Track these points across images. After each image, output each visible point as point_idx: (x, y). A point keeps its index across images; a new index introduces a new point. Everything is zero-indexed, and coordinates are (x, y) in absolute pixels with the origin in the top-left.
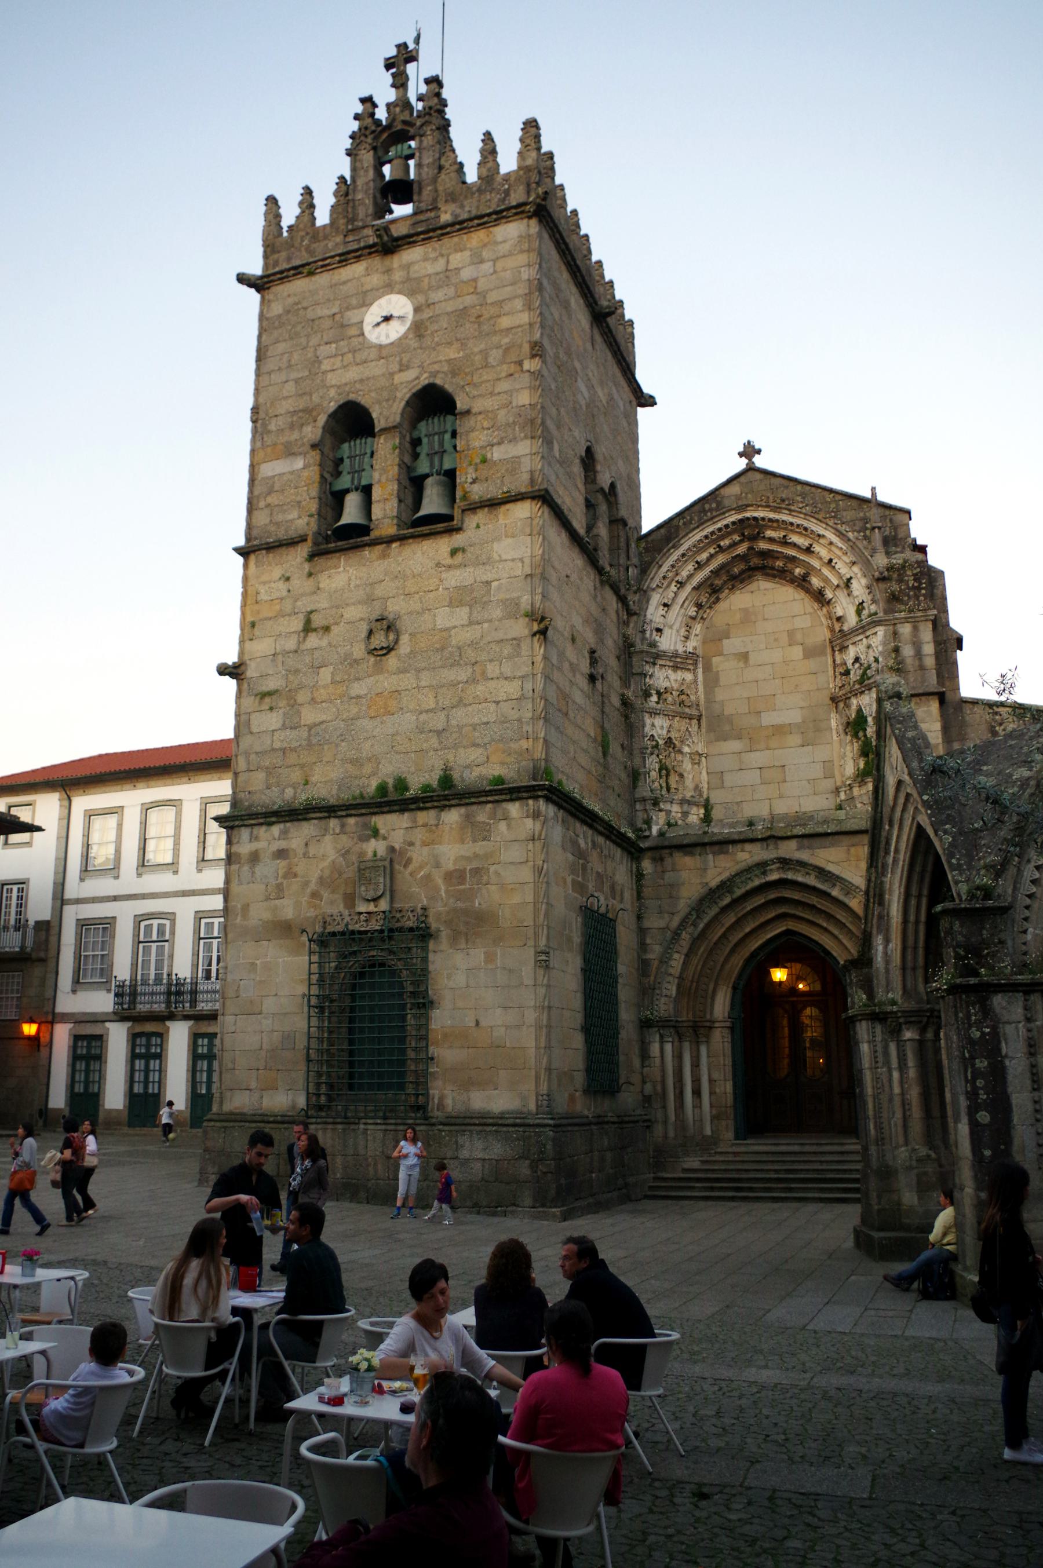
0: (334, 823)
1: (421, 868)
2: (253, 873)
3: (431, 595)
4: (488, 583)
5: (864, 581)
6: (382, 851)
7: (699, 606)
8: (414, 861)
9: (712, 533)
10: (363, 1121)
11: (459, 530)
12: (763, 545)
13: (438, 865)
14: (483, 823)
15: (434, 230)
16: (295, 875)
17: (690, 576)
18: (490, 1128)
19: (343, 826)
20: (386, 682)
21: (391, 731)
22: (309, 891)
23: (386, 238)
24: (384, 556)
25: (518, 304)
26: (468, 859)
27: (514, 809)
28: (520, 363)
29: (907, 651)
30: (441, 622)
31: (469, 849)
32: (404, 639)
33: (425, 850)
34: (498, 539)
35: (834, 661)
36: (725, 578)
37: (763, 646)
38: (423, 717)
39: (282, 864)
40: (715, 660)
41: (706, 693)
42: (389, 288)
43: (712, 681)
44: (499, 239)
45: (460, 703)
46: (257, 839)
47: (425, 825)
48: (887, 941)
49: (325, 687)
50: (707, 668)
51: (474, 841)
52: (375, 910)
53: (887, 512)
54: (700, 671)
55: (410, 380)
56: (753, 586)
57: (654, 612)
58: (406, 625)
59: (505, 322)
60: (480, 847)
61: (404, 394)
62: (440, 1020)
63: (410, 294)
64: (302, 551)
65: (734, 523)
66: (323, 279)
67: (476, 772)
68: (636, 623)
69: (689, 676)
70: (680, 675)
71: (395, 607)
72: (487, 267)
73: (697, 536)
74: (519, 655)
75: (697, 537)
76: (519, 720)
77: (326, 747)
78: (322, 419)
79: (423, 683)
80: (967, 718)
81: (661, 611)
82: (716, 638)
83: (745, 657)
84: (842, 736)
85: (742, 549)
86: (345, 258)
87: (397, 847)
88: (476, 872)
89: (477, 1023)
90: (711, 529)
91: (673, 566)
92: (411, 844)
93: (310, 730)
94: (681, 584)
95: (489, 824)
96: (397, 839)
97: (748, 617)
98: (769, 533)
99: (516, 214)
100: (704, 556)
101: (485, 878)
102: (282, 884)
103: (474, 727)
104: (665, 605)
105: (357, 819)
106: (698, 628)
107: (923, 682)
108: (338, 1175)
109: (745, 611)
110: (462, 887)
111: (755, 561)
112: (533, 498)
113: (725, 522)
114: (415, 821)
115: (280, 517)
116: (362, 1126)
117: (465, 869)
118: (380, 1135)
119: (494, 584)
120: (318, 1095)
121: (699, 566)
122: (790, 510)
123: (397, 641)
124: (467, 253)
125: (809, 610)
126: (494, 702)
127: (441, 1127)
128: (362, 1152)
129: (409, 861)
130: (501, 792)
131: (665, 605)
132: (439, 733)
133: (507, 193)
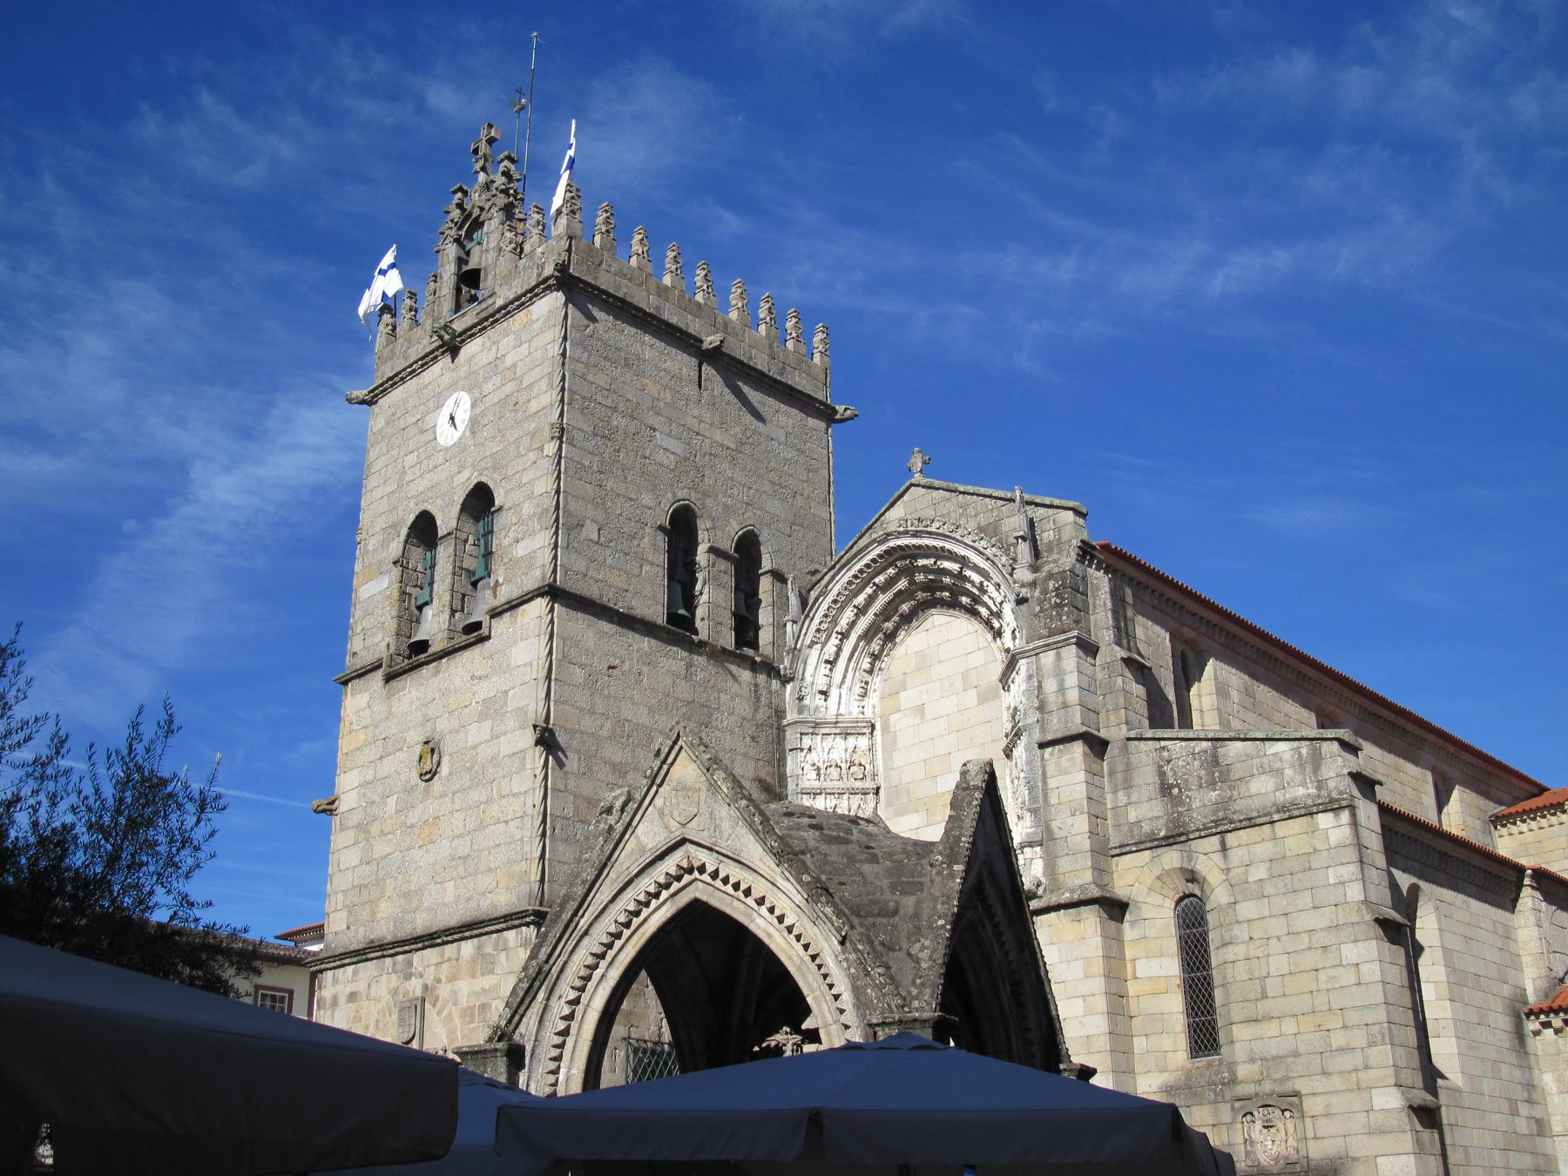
1: (444, 1006)
3: (466, 711)
4: (506, 692)
7: (876, 657)
9: (861, 571)
11: (488, 638)
12: (920, 578)
15: (486, 319)
17: (852, 625)
20: (432, 808)
21: (431, 860)
23: (447, 337)
24: (437, 672)
25: (543, 385)
28: (541, 449)
29: (1050, 686)
30: (472, 740)
32: (445, 760)
34: (515, 643)
36: (896, 618)
37: (938, 695)
40: (893, 718)
41: (885, 761)
42: (453, 387)
43: (891, 746)
44: (535, 317)
45: (482, 826)
47: (449, 960)
49: (391, 817)
50: (885, 729)
53: (1051, 511)
54: (878, 732)
55: (463, 483)
56: (928, 624)
57: (814, 672)
58: (448, 747)
59: (534, 406)
61: (460, 497)
63: (469, 391)
64: (378, 676)
65: (880, 556)
66: (412, 384)
68: (793, 688)
69: (863, 742)
70: (851, 739)
71: (443, 725)
72: (524, 349)
73: (845, 576)
74: (524, 769)
75: (846, 579)
76: (521, 840)
78: (404, 532)
80: (1133, 759)
81: (824, 669)
82: (892, 694)
83: (920, 709)
85: (902, 584)
86: (427, 360)
90: (857, 567)
91: (826, 616)
92: (439, 981)
94: (844, 636)
97: (924, 662)
98: (921, 562)
99: (544, 290)
100: (860, 599)
103: (489, 849)
104: (827, 662)
106: (877, 682)
107: (1067, 722)
109: (920, 654)
111: (920, 595)
112: (542, 595)
113: (870, 556)
114: (442, 956)
115: (369, 642)
121: (861, 611)
122: (930, 533)
123: (439, 764)
124: (512, 336)
125: (983, 643)
130: (511, 920)
131: (827, 662)
132: (465, 858)
133: (542, 266)
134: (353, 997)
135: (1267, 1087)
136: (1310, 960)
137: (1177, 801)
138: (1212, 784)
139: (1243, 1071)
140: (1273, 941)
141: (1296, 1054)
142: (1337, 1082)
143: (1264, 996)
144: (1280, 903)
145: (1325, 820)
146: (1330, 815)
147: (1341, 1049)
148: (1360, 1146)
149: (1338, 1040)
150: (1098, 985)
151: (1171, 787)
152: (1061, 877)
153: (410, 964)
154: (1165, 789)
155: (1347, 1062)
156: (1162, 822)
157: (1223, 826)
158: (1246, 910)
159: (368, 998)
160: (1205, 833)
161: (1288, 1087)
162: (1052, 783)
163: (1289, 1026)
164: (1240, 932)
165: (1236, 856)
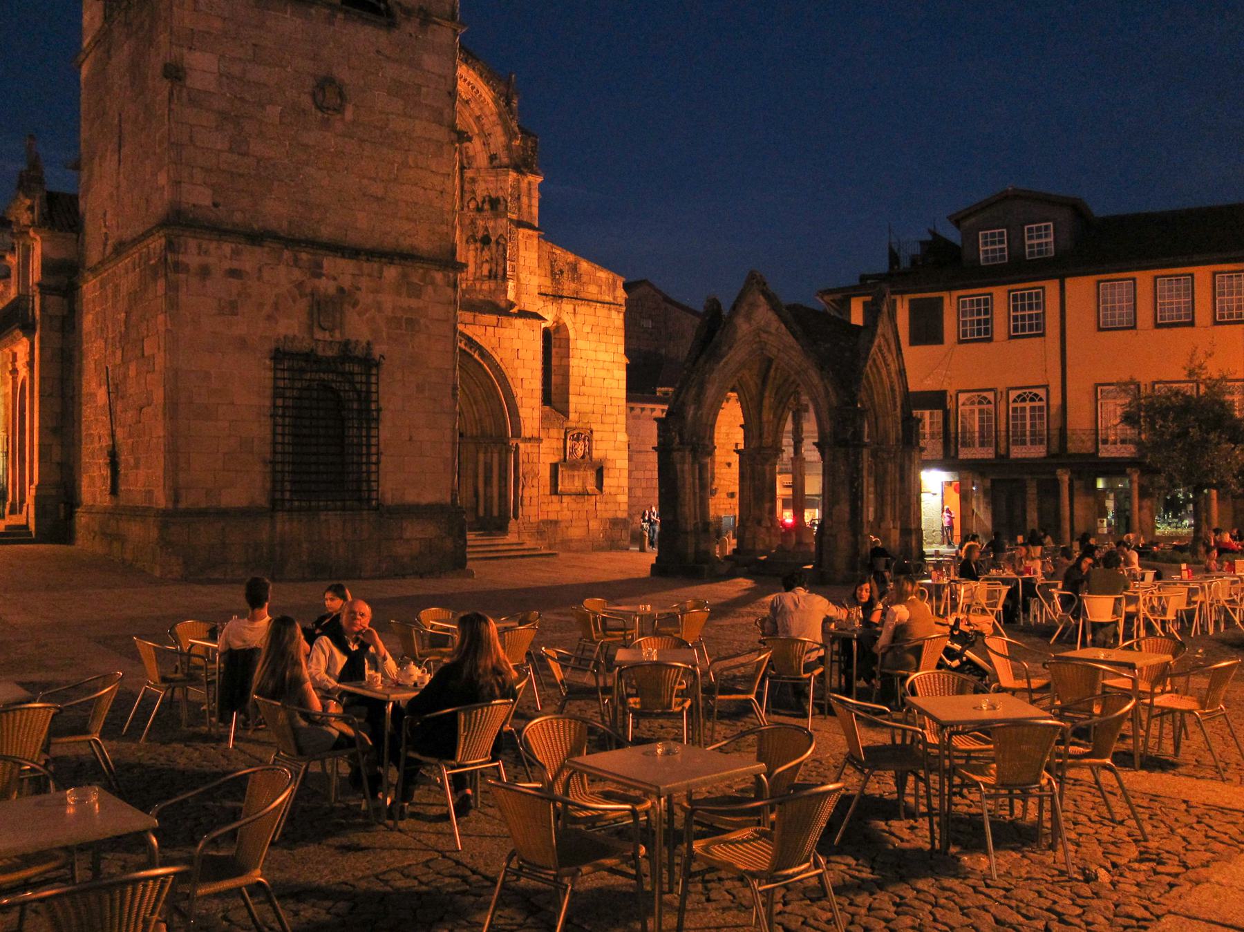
0: (287, 254)
1: (366, 311)
2: (204, 286)
6: (332, 290)
19: (296, 261)
27: (439, 276)
31: (406, 302)
33: (371, 296)
38: (365, 181)
39: (235, 281)
46: (206, 252)
51: (410, 297)
60: (414, 303)
62: (385, 432)
71: (342, 74)
77: (276, 183)
88: (410, 321)
96: (346, 282)
119: (424, 90)
120: (283, 492)
129: (355, 305)
134: (234, 273)
135: (580, 425)
138: (573, 280)
139: (572, 416)
142: (607, 427)
144: (593, 346)
148: (611, 455)
149: (609, 410)
154: (553, 273)
155: (612, 419)
159: (259, 279)
162: (522, 253)
163: (591, 400)
165: (580, 318)
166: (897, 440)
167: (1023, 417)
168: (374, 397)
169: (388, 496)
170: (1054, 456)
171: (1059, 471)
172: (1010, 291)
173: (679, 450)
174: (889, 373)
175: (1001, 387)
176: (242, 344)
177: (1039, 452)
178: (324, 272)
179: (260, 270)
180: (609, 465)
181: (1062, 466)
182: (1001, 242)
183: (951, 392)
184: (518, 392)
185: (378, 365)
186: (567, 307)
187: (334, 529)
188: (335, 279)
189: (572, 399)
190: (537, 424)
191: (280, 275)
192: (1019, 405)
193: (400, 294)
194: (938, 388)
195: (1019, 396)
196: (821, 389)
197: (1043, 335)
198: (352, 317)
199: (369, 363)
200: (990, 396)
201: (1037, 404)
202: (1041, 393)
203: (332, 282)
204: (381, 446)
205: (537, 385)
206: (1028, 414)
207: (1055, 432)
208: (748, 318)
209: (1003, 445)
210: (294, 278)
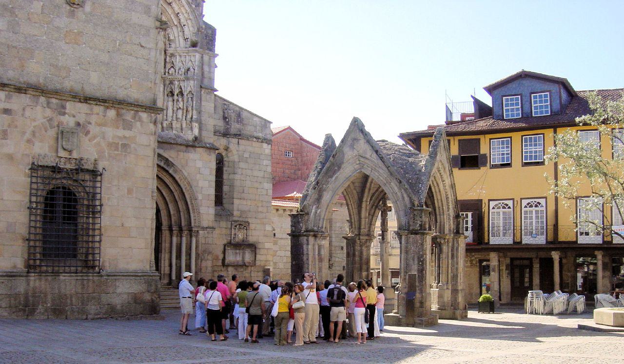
0: (42, 99)
1: (95, 137)
5: (191, 29)
8: (91, 133)
10: (63, 274)
13: (104, 138)
14: (129, 121)
16: (16, 127)
18: (131, 278)
19: (48, 103)
22: (25, 138)
26: (120, 138)
31: (121, 132)
33: (98, 129)
35: (165, 60)
48: (318, 208)
51: (124, 129)
52: (70, 157)
60: (127, 133)
62: (106, 220)
67: (125, 92)
79: (98, 33)
84: (166, 96)
87: (81, 123)
88: (125, 146)
89: (122, 226)
92: (90, 123)
93: (26, 38)
95: (131, 121)
96: (82, 119)
101: (129, 150)
102: (7, 130)
105: (57, 101)
108: (49, 305)
110: (116, 152)
114: (91, 110)
116: (61, 277)
117: (119, 143)
118: (74, 282)
126: (136, 57)
127: (106, 277)
128: (63, 291)
129: (88, 133)
135: (241, 219)
136: (256, 185)
137: (227, 123)
138: (238, 122)
139: (236, 213)
140: (248, 177)
141: (250, 211)
143: (243, 192)
145: (265, 145)
146: (267, 145)
147: (260, 212)
148: (261, 239)
149: (260, 209)
150: (213, 178)
151: (226, 118)
152: (203, 138)
153: (64, 107)
154: (225, 118)
156: (222, 128)
157: (238, 135)
158: (242, 165)
159: (23, 115)
160: (235, 135)
161: (247, 220)
163: (249, 203)
164: (239, 171)
165: (241, 148)
166: (450, 230)
167: (531, 218)
168: (98, 196)
169: (107, 264)
170: (551, 243)
171: (553, 253)
172: (522, 136)
173: (305, 235)
174: (444, 186)
175: (517, 199)
176: (10, 157)
177: (541, 240)
178: (67, 111)
179: (24, 109)
180: (259, 246)
181: (555, 249)
182: (517, 104)
183: (485, 201)
184: (200, 197)
185: (101, 175)
186: (235, 141)
187: (68, 283)
188: (74, 116)
189: (236, 202)
190: (212, 218)
191: (36, 114)
192: (528, 209)
193: (118, 128)
194: (476, 198)
195: (528, 204)
196: (399, 194)
197: (542, 163)
198: (85, 140)
199: (95, 173)
200: (510, 203)
201: (539, 209)
202: (543, 201)
203: (72, 118)
204: (103, 230)
205: (212, 191)
206: (534, 215)
207: (551, 227)
208: (352, 147)
209: (518, 235)
210: (46, 115)
